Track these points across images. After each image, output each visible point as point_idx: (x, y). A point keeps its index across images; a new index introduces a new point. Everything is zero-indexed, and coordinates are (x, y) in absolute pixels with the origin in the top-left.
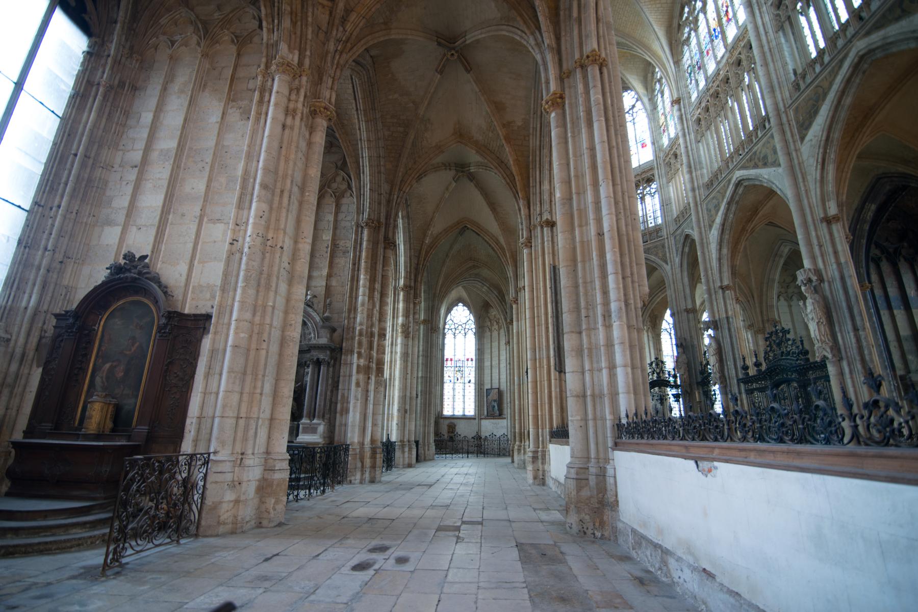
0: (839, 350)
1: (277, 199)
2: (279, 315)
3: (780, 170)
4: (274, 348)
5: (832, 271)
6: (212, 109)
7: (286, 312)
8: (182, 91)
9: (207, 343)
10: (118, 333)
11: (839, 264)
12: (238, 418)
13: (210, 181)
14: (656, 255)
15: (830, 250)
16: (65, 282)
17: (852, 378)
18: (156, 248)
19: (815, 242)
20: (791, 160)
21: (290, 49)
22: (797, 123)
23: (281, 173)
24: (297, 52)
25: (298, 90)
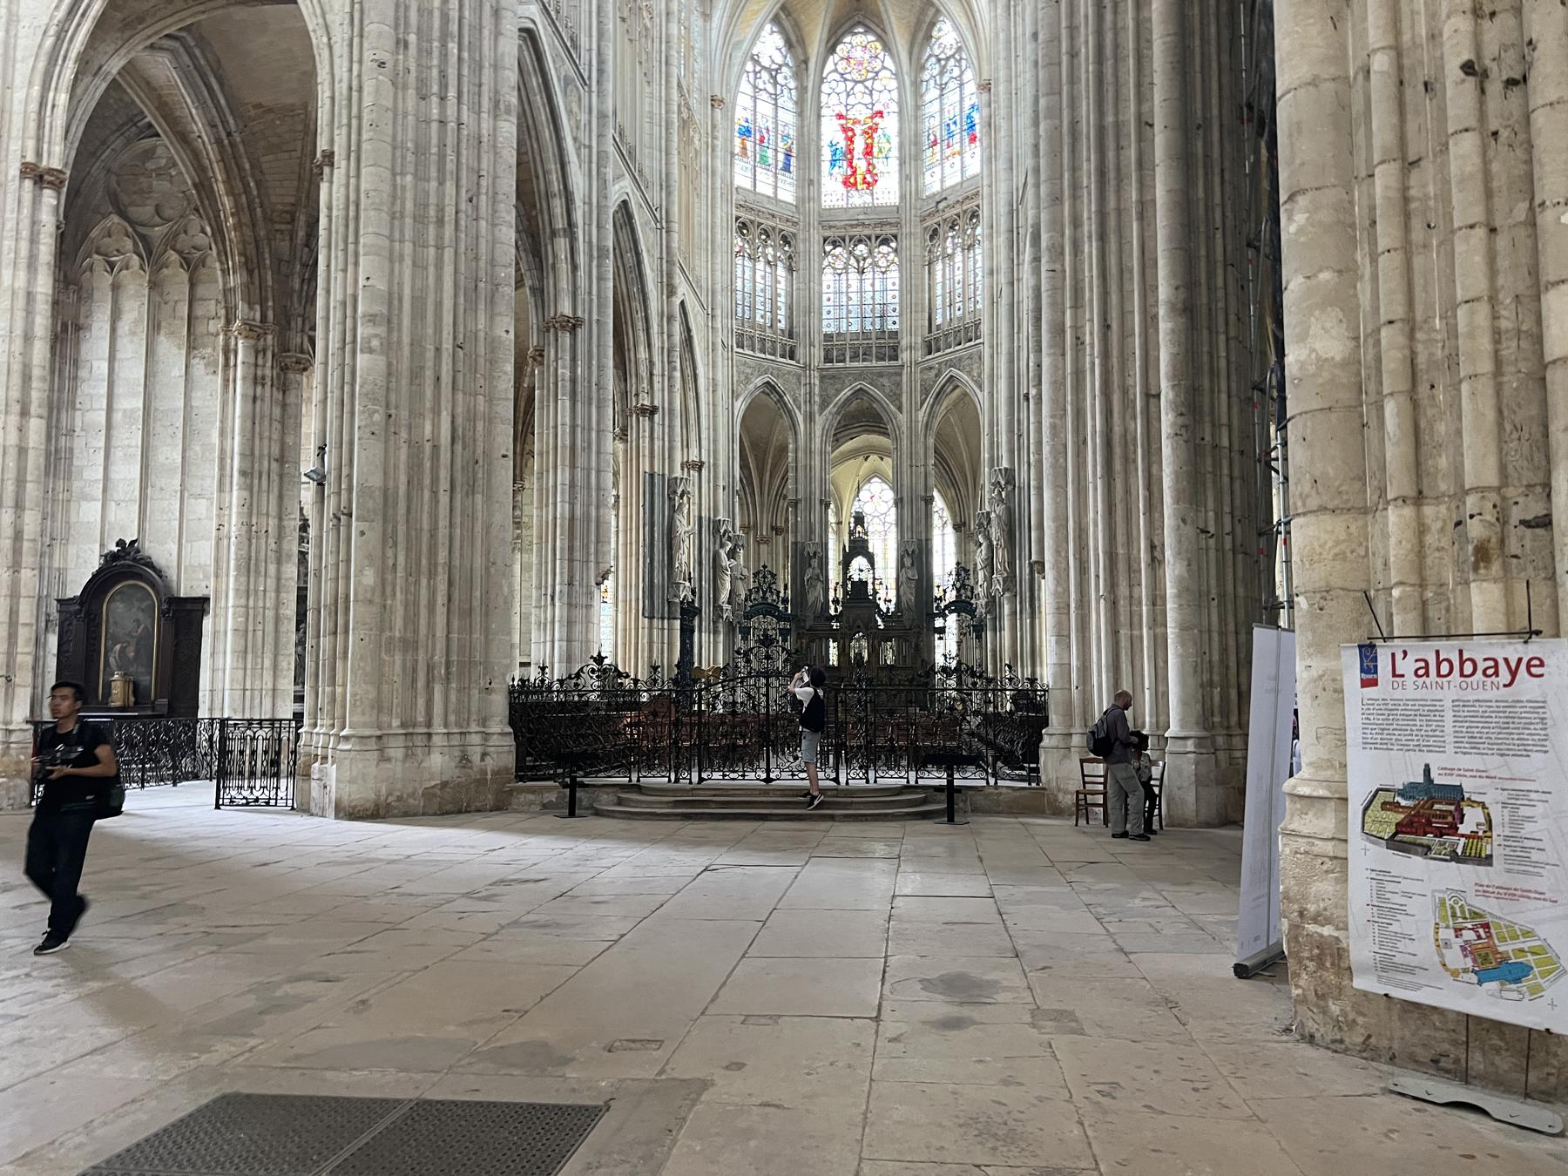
1: (256, 482)
2: (271, 595)
4: (270, 627)
6: (172, 353)
7: (278, 591)
8: (133, 333)
9: (207, 623)
10: (126, 617)
12: (244, 690)
13: (184, 451)
14: (969, 373)
16: (56, 565)
18: (141, 528)
21: (250, 306)
23: (257, 453)
24: (258, 307)
25: (264, 351)
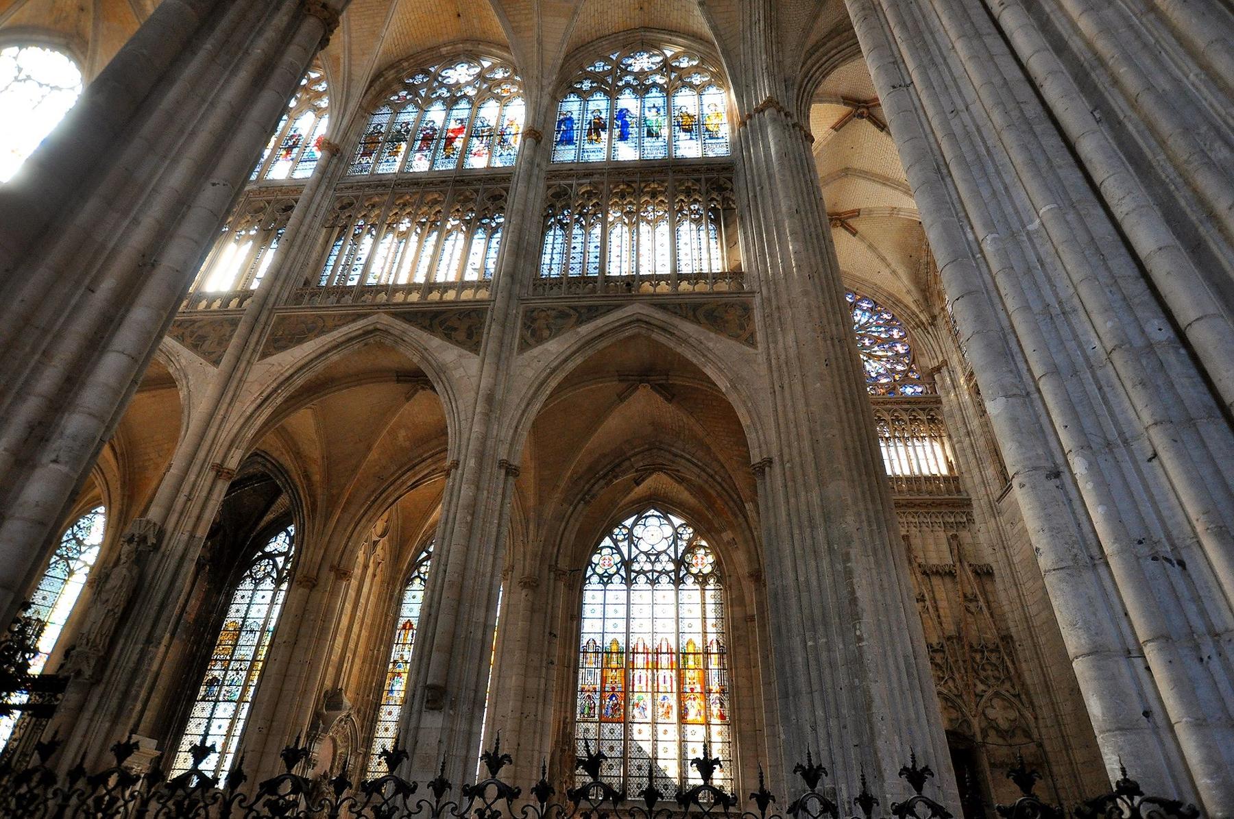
0: (103, 671)
3: (213, 370)
5: (177, 541)
11: (192, 536)
15: (195, 512)
17: (91, 720)
19: (186, 489)
20: (235, 368)
22: (272, 334)
